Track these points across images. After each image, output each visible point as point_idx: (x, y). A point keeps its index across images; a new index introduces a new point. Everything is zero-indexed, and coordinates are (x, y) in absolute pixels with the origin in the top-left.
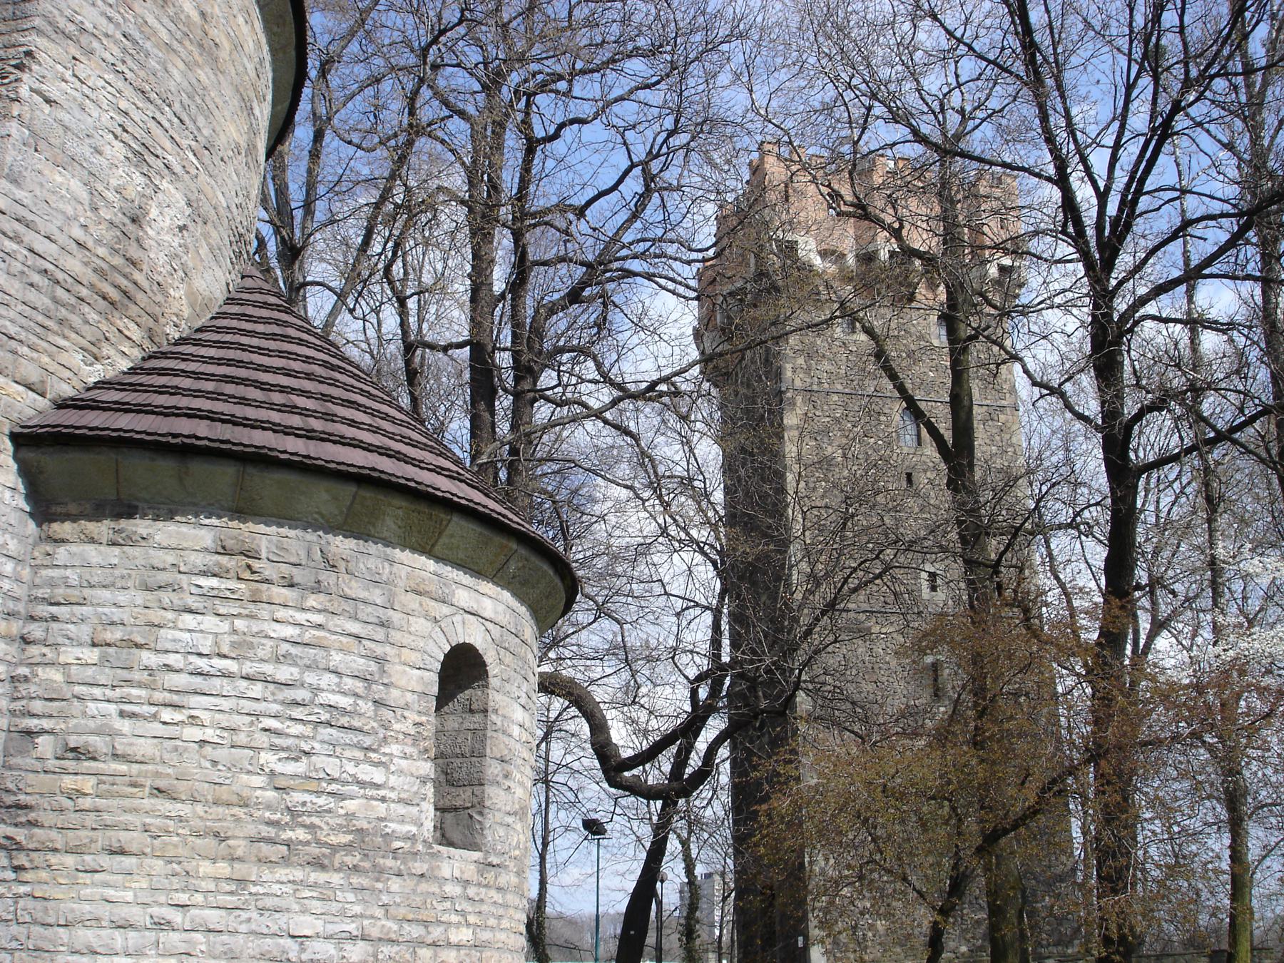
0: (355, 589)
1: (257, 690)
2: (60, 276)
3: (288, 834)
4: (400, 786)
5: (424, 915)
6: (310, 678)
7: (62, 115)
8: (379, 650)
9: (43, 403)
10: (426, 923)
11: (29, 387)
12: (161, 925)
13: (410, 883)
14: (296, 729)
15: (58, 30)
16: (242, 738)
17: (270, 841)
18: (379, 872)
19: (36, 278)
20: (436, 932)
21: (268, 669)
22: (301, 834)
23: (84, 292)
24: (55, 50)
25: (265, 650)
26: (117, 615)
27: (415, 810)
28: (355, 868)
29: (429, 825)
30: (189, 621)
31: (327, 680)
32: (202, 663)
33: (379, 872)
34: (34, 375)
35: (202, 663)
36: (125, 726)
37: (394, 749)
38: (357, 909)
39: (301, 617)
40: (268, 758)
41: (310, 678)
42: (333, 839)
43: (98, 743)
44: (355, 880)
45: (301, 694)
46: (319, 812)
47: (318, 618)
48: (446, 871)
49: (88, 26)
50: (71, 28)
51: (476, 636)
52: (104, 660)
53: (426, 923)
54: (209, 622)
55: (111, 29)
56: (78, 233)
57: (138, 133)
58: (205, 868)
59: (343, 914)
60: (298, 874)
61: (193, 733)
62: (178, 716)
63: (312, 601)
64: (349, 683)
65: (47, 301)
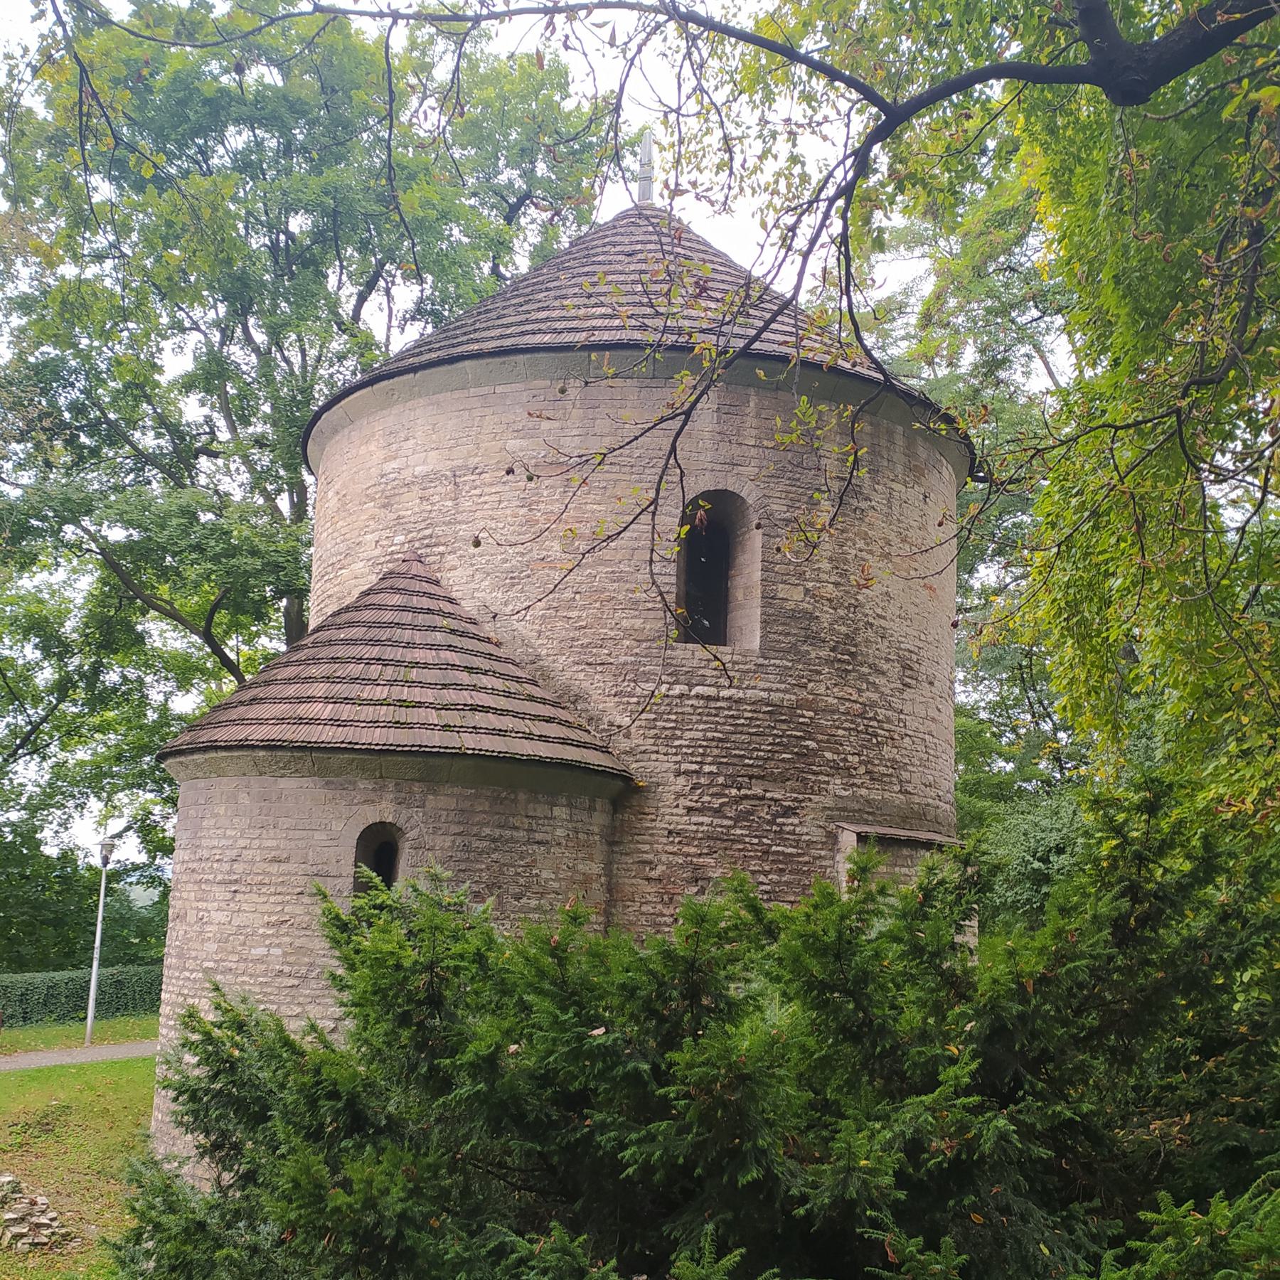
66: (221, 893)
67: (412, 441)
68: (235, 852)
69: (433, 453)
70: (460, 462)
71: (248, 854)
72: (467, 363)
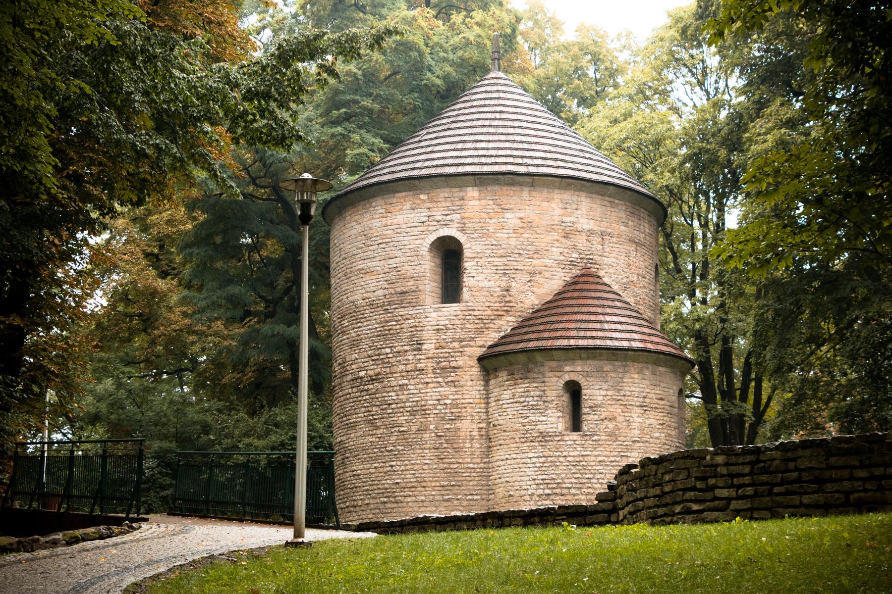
1: (517, 405)
4: (555, 420)
6: (527, 399)
7: (476, 278)
9: (485, 349)
12: (507, 459)
18: (546, 441)
19: (477, 321)
20: (565, 454)
31: (531, 399)
33: (546, 441)
34: (481, 343)
37: (549, 411)
40: (521, 420)
41: (527, 399)
43: (496, 423)
45: (526, 404)
48: (566, 438)
50: (475, 255)
54: (509, 392)
56: (487, 304)
57: (502, 268)
60: (528, 444)
66: (638, 410)
67: (579, 212)
68: (645, 394)
69: (592, 221)
70: (603, 229)
71: (650, 395)
72: (612, 187)
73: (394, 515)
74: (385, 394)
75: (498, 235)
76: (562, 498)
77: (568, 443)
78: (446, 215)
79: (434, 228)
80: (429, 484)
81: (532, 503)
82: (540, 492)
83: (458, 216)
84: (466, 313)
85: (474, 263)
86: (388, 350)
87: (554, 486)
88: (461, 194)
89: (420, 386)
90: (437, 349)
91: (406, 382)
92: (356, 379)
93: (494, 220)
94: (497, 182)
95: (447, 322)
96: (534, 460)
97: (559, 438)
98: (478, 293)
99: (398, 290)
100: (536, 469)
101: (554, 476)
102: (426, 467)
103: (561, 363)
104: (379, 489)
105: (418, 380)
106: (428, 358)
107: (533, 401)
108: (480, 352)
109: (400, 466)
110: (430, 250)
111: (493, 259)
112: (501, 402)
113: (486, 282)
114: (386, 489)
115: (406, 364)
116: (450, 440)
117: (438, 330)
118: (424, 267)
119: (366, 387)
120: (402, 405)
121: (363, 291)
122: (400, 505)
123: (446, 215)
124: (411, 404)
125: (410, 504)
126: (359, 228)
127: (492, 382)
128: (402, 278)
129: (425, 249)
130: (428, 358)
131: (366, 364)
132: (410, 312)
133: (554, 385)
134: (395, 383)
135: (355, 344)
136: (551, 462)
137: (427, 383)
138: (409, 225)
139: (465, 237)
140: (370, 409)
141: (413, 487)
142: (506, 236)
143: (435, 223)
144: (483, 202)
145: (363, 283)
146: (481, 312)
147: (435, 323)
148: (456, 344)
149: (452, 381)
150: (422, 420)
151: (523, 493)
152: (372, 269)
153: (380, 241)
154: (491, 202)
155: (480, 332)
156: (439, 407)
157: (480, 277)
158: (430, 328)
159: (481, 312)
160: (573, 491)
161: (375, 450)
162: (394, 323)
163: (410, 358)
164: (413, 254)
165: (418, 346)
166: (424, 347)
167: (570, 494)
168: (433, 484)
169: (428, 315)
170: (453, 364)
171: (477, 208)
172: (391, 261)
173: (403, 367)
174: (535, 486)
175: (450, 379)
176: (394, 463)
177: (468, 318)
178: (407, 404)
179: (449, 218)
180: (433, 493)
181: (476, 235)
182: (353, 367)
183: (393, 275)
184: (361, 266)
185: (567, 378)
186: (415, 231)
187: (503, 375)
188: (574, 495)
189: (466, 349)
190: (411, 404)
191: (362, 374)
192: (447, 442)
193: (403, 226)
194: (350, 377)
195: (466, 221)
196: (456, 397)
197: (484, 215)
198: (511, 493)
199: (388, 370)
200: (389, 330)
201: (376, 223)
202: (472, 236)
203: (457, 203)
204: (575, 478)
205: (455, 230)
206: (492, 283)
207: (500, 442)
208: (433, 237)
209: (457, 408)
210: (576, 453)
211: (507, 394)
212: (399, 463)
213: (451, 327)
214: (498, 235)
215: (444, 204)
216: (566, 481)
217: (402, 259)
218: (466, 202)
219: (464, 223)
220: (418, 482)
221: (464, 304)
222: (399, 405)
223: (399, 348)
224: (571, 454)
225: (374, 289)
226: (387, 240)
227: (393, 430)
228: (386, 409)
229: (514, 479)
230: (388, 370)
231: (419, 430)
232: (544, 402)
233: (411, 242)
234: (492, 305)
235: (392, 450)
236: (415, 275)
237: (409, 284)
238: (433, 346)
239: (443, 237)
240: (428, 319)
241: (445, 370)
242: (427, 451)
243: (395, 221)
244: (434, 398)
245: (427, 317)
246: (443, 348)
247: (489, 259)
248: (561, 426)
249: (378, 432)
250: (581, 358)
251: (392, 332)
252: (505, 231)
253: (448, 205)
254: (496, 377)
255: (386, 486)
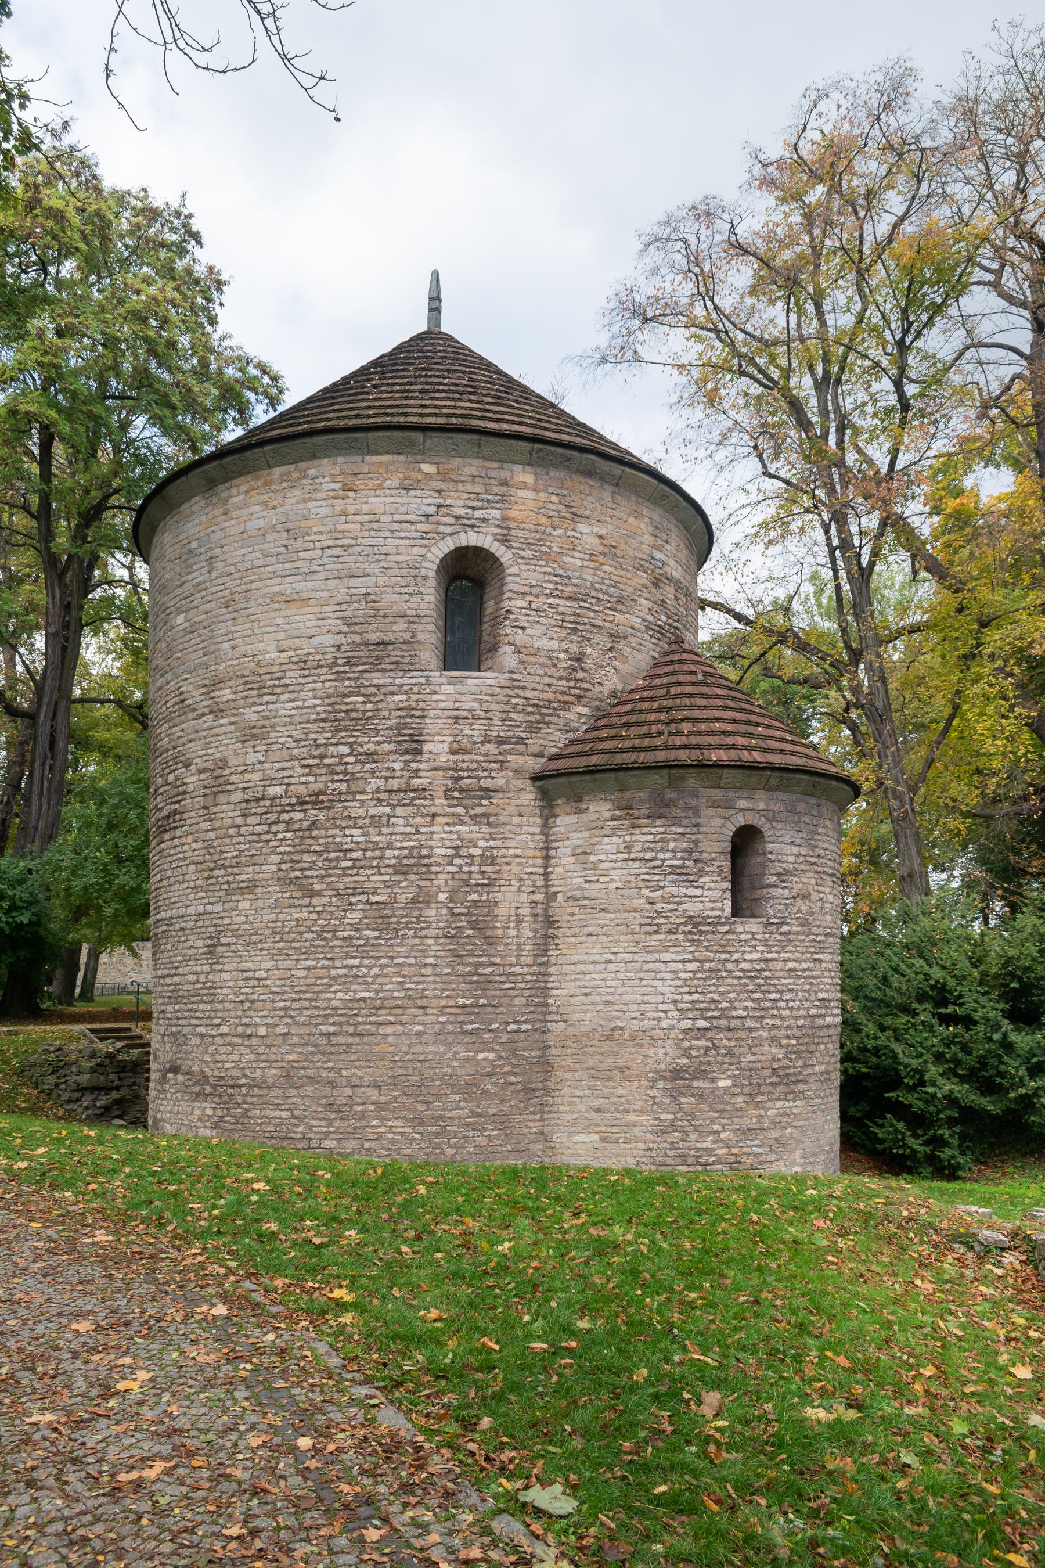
0: (679, 813)
1: (637, 864)
2: (541, 703)
3: (656, 921)
4: (712, 895)
5: (728, 949)
6: (661, 856)
7: (528, 631)
8: (694, 837)
10: (730, 952)
11: (535, 755)
12: (609, 961)
13: (719, 936)
14: (657, 877)
15: (518, 593)
16: (633, 885)
17: (650, 925)
18: (701, 933)
19: (530, 709)
20: (736, 956)
21: (641, 855)
22: (662, 921)
23: (556, 705)
24: (519, 603)
25: (638, 847)
26: (579, 842)
27: (719, 905)
28: (690, 932)
29: (728, 911)
30: (606, 840)
31: (668, 855)
32: (614, 857)
33: (701, 933)
35: (614, 857)
36: (587, 886)
37: (707, 879)
38: (692, 949)
39: (654, 830)
40: (645, 892)
42: (678, 921)
44: (690, 937)
46: (670, 911)
47: (662, 829)
48: (740, 928)
49: (534, 583)
50: (526, 589)
51: (752, 819)
52: (577, 861)
53: (730, 952)
54: (615, 839)
55: (547, 578)
56: (547, 680)
57: (572, 618)
58: (623, 938)
59: (684, 951)
60: (662, 937)
61: (615, 885)
62: (606, 879)
63: (658, 822)
64: (679, 855)
65: (538, 717)
73: (353, 1057)
74: (336, 831)
75: (567, 559)
76: (730, 1035)
77: (743, 937)
78: (474, 509)
79: (449, 530)
80: (434, 1002)
81: (669, 1042)
82: (688, 1024)
83: (497, 514)
84: (511, 693)
85: (524, 604)
86: (344, 750)
87: (715, 1013)
88: (504, 474)
89: (418, 820)
90: (453, 753)
91: (388, 810)
92: (257, 800)
93: (559, 532)
94: (565, 464)
95: (475, 705)
96: (673, 966)
97: (726, 928)
98: (531, 659)
99: (373, 637)
100: (680, 983)
101: (716, 997)
102: (428, 971)
103: (731, 793)
104: (317, 1008)
105: (414, 809)
106: (436, 769)
107: (674, 858)
108: (536, 765)
109: (370, 967)
110: (438, 572)
111: (557, 601)
112: (593, 858)
113: (545, 641)
114: (335, 1009)
115: (386, 778)
116: (477, 922)
117: (457, 718)
118: (427, 598)
119: (285, 817)
120: (378, 853)
121: (282, 635)
122: (366, 1039)
123: (474, 509)
124: (396, 853)
125: (391, 1039)
126: (273, 518)
127: (564, 822)
128: (377, 614)
129: (430, 568)
130: (436, 769)
131: (285, 773)
132: (398, 682)
133: (717, 832)
134: (361, 812)
135: (252, 735)
136: (711, 970)
137: (434, 815)
138: (396, 517)
139: (509, 554)
140: (296, 858)
141: (398, 1007)
142: (578, 563)
143: (452, 521)
144: (542, 495)
145: (279, 621)
146: (536, 693)
147: (451, 705)
148: (491, 748)
149: (482, 815)
150: (422, 883)
151: (647, 1024)
152: (306, 595)
153: (330, 543)
154: (554, 498)
155: (533, 728)
156: (457, 861)
157: (535, 631)
158: (440, 712)
159: (536, 693)
160: (749, 1023)
161: (310, 936)
162: (360, 699)
163: (397, 766)
164: (404, 572)
165: (413, 745)
166: (427, 747)
167: (743, 1028)
168: (443, 1003)
169: (437, 689)
170: (486, 783)
171: (531, 505)
172: (355, 582)
173: (381, 783)
174: (676, 1014)
175: (478, 810)
176: (356, 962)
177: (514, 701)
178: (388, 853)
179: (478, 514)
180: (442, 1019)
181: (528, 553)
182: (248, 776)
183: (359, 609)
184: (277, 589)
185: (741, 820)
186: (411, 531)
187: (600, 809)
188: (751, 1030)
189: (509, 758)
190: (396, 853)
191: (279, 790)
192: (472, 925)
193: (383, 518)
194: (238, 796)
195: (512, 525)
196: (491, 843)
197: (544, 520)
198: (622, 1025)
199: (343, 787)
200: (347, 711)
201: (319, 508)
202: (521, 553)
203: (496, 490)
204: (753, 1000)
205: (490, 538)
206: (555, 643)
207: (590, 930)
208: (448, 546)
209: (493, 864)
210: (756, 956)
211: (609, 846)
212: (366, 962)
213: (482, 713)
214: (567, 559)
215: (469, 488)
216: (737, 1004)
217: (381, 581)
218: (512, 491)
219: (508, 528)
220: (410, 997)
221: (507, 675)
222: (369, 854)
223: (371, 747)
224: (748, 956)
225: (312, 632)
226: (346, 542)
227: (353, 900)
228: (337, 859)
229: (626, 998)
230: (343, 787)
231: (414, 901)
232: (696, 861)
233: (403, 550)
234: (555, 682)
235: (351, 938)
236: (409, 612)
237: (395, 627)
238: (446, 747)
239: (467, 548)
240: (436, 697)
241: (469, 794)
242: (431, 942)
243: (365, 508)
244: (448, 844)
245: (435, 692)
246: (466, 752)
247: (551, 601)
248: (728, 904)
249: (316, 901)
250: (766, 788)
251: (354, 715)
252: (577, 554)
253: (477, 489)
254: (579, 811)
255: (334, 1003)
